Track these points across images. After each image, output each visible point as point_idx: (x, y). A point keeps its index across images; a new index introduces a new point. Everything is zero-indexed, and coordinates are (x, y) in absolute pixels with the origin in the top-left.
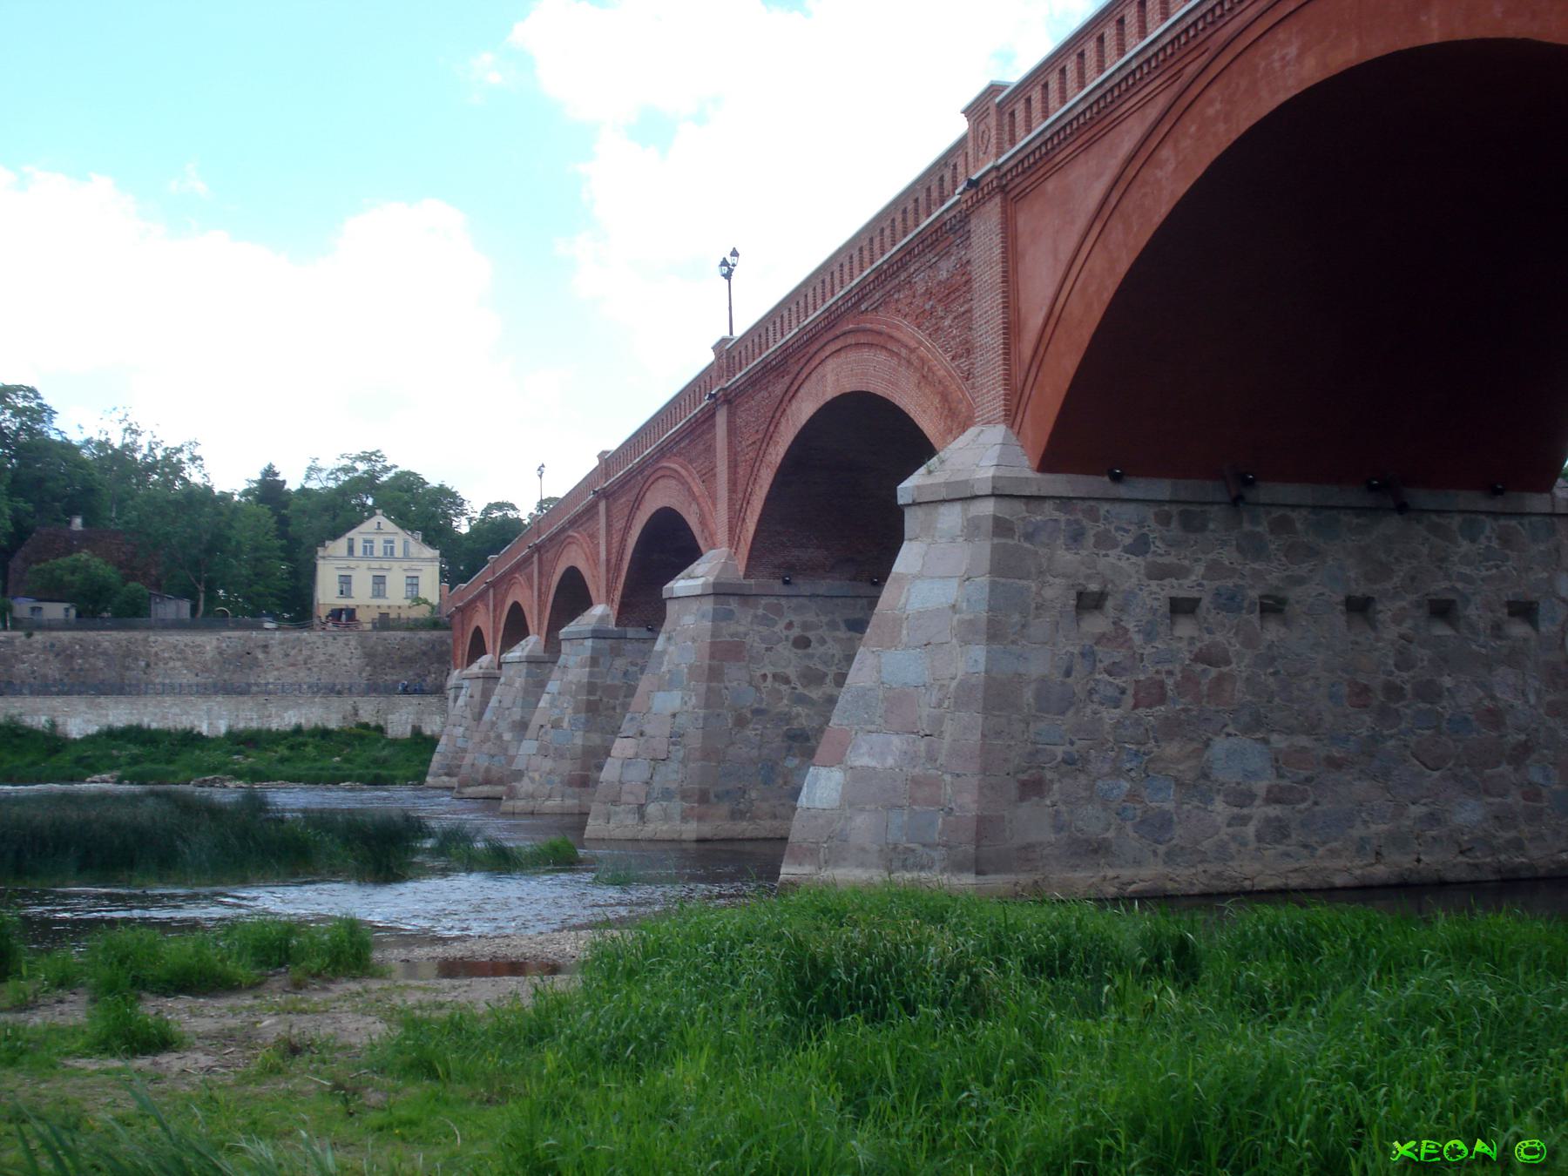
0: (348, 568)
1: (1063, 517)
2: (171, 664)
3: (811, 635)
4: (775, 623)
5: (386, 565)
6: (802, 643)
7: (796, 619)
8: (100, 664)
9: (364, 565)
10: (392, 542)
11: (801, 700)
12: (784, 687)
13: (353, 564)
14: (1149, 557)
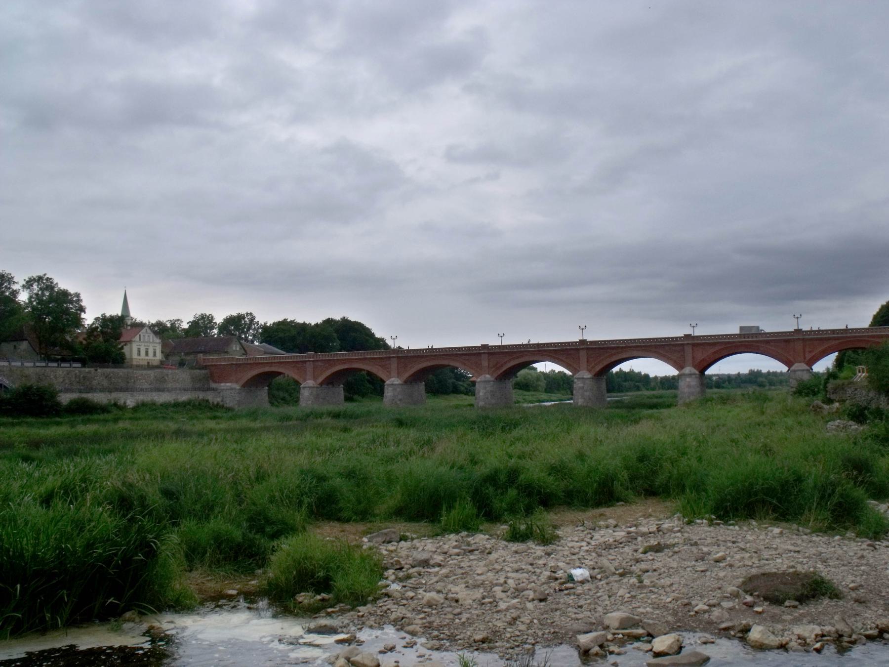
0: (139, 345)
2: (141, 381)
5: (148, 344)
8: (120, 381)
9: (143, 344)
13: (140, 344)
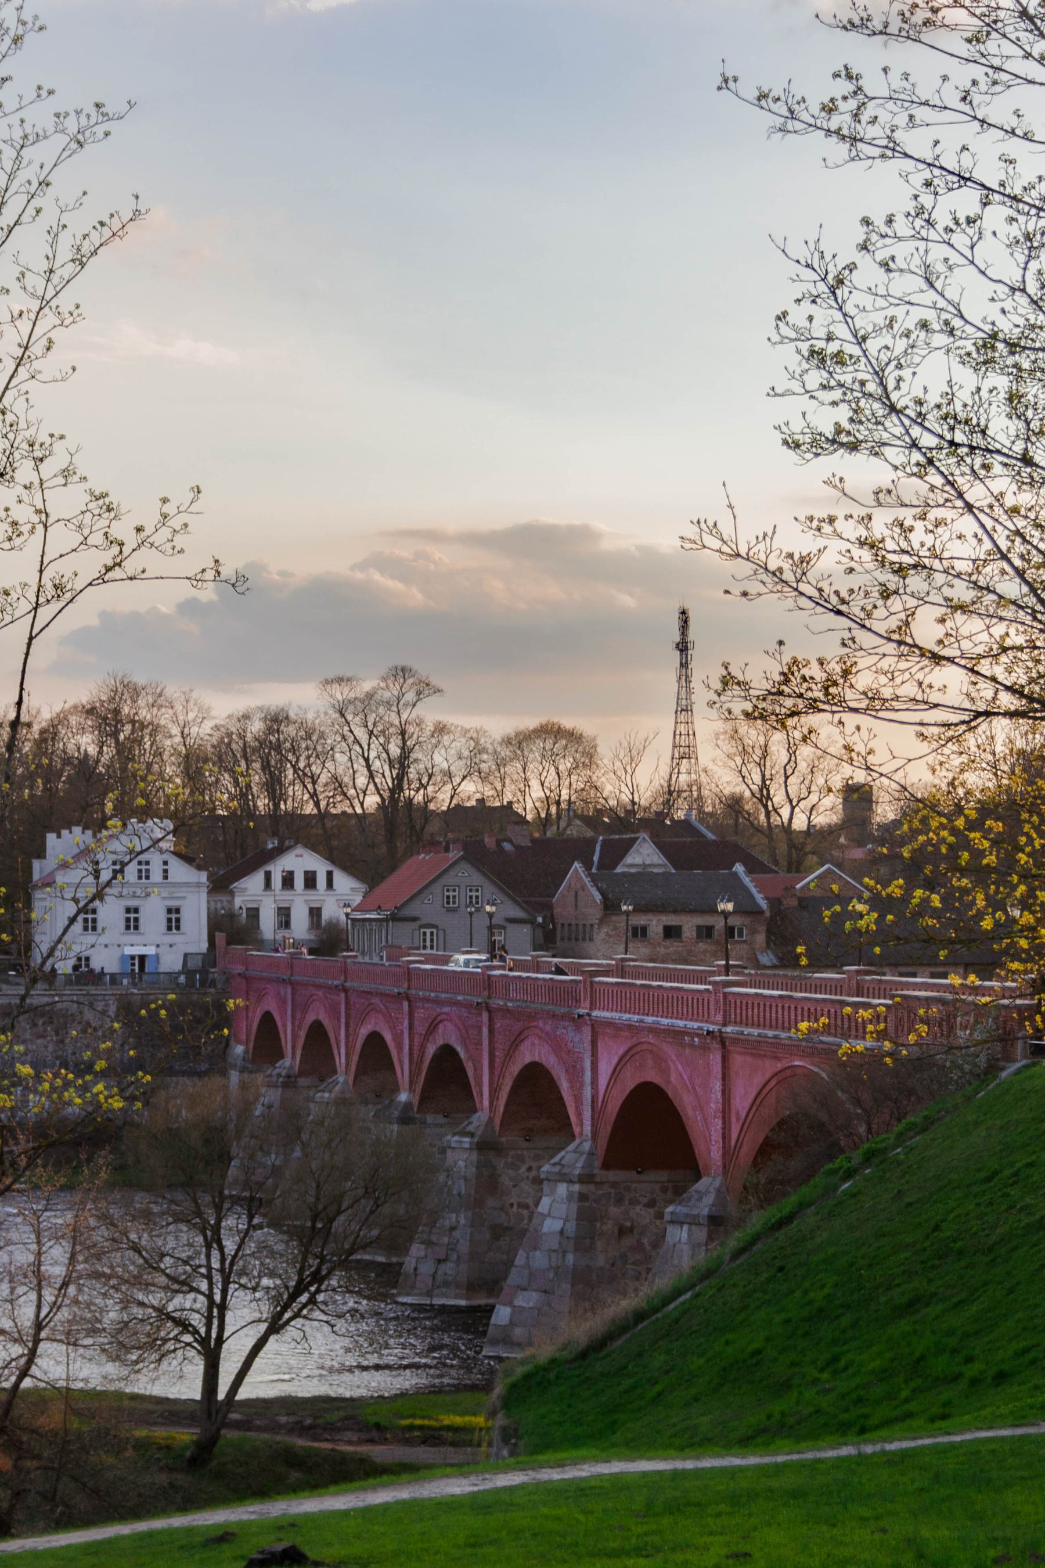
1: (613, 1191)
4: (519, 1168)
7: (534, 1165)
10: (147, 863)
14: (656, 1209)
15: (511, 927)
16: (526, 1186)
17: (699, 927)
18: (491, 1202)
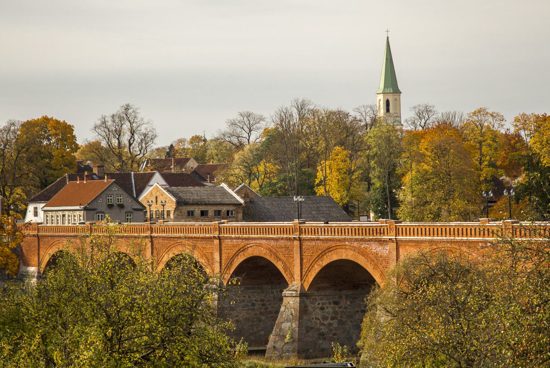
3: (324, 306)
4: (315, 303)
6: (322, 309)
7: (320, 302)
11: (322, 324)
12: (318, 321)
15: (135, 212)
16: (318, 311)
17: (215, 211)
18: (305, 318)
